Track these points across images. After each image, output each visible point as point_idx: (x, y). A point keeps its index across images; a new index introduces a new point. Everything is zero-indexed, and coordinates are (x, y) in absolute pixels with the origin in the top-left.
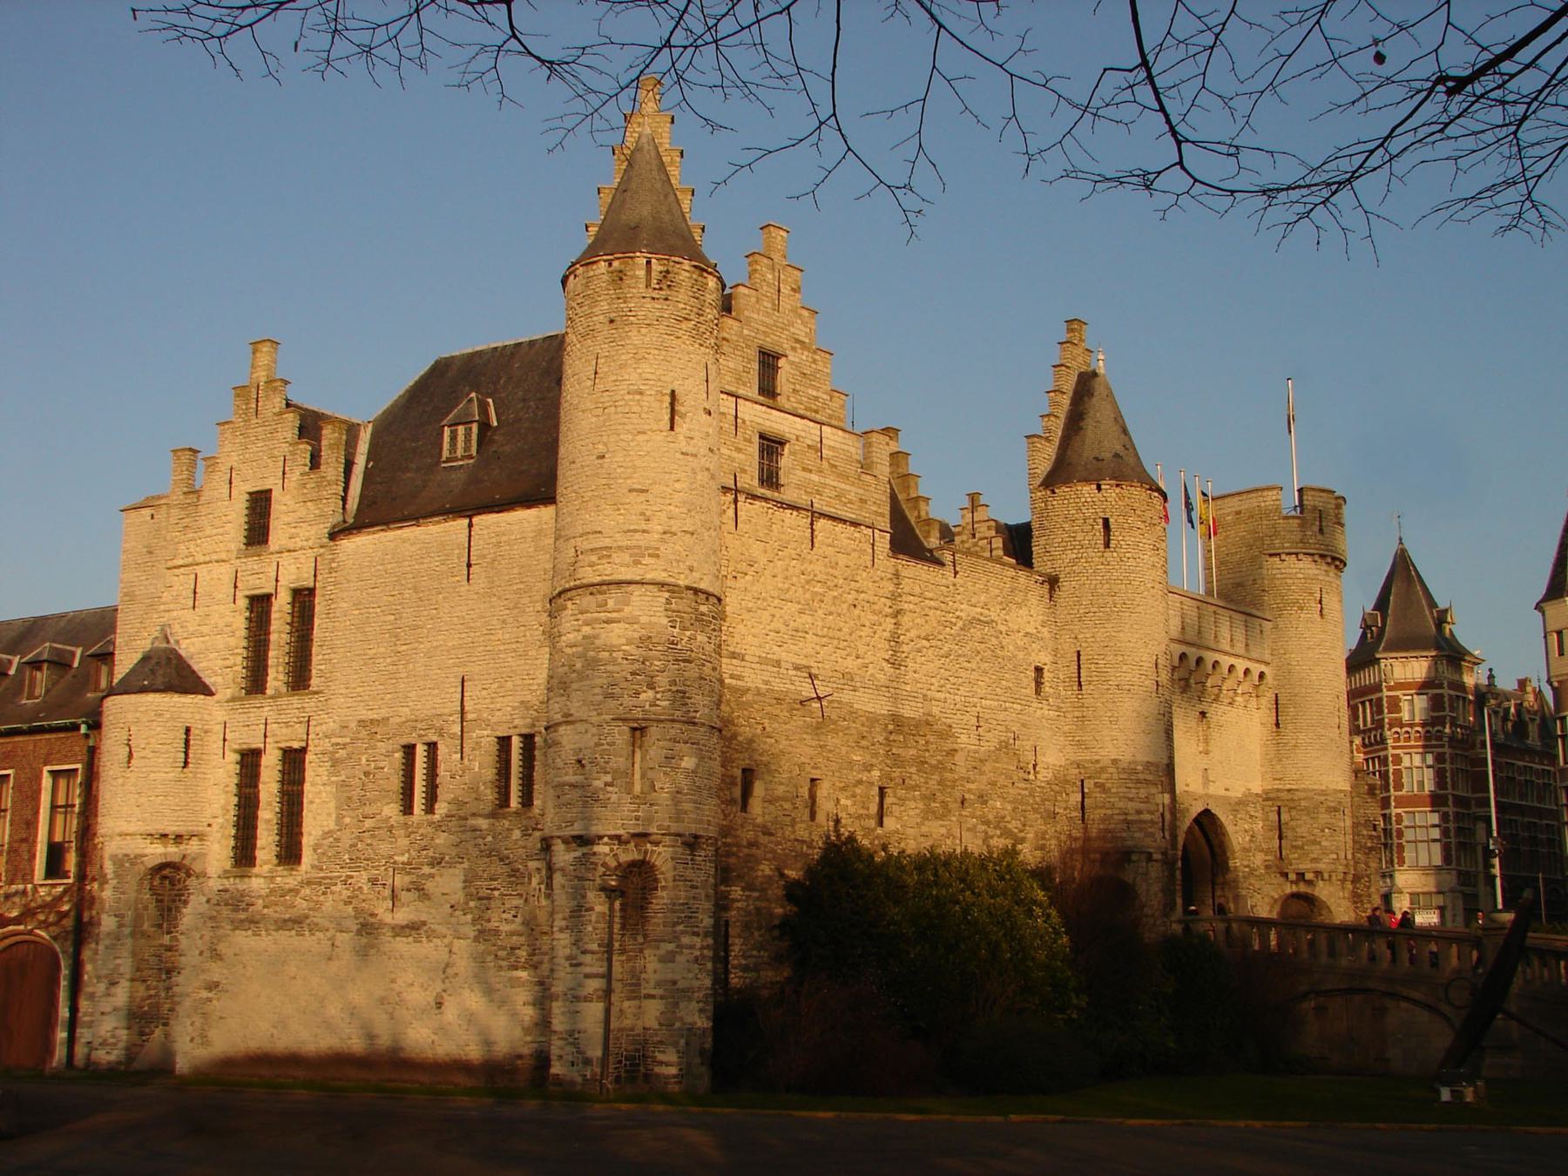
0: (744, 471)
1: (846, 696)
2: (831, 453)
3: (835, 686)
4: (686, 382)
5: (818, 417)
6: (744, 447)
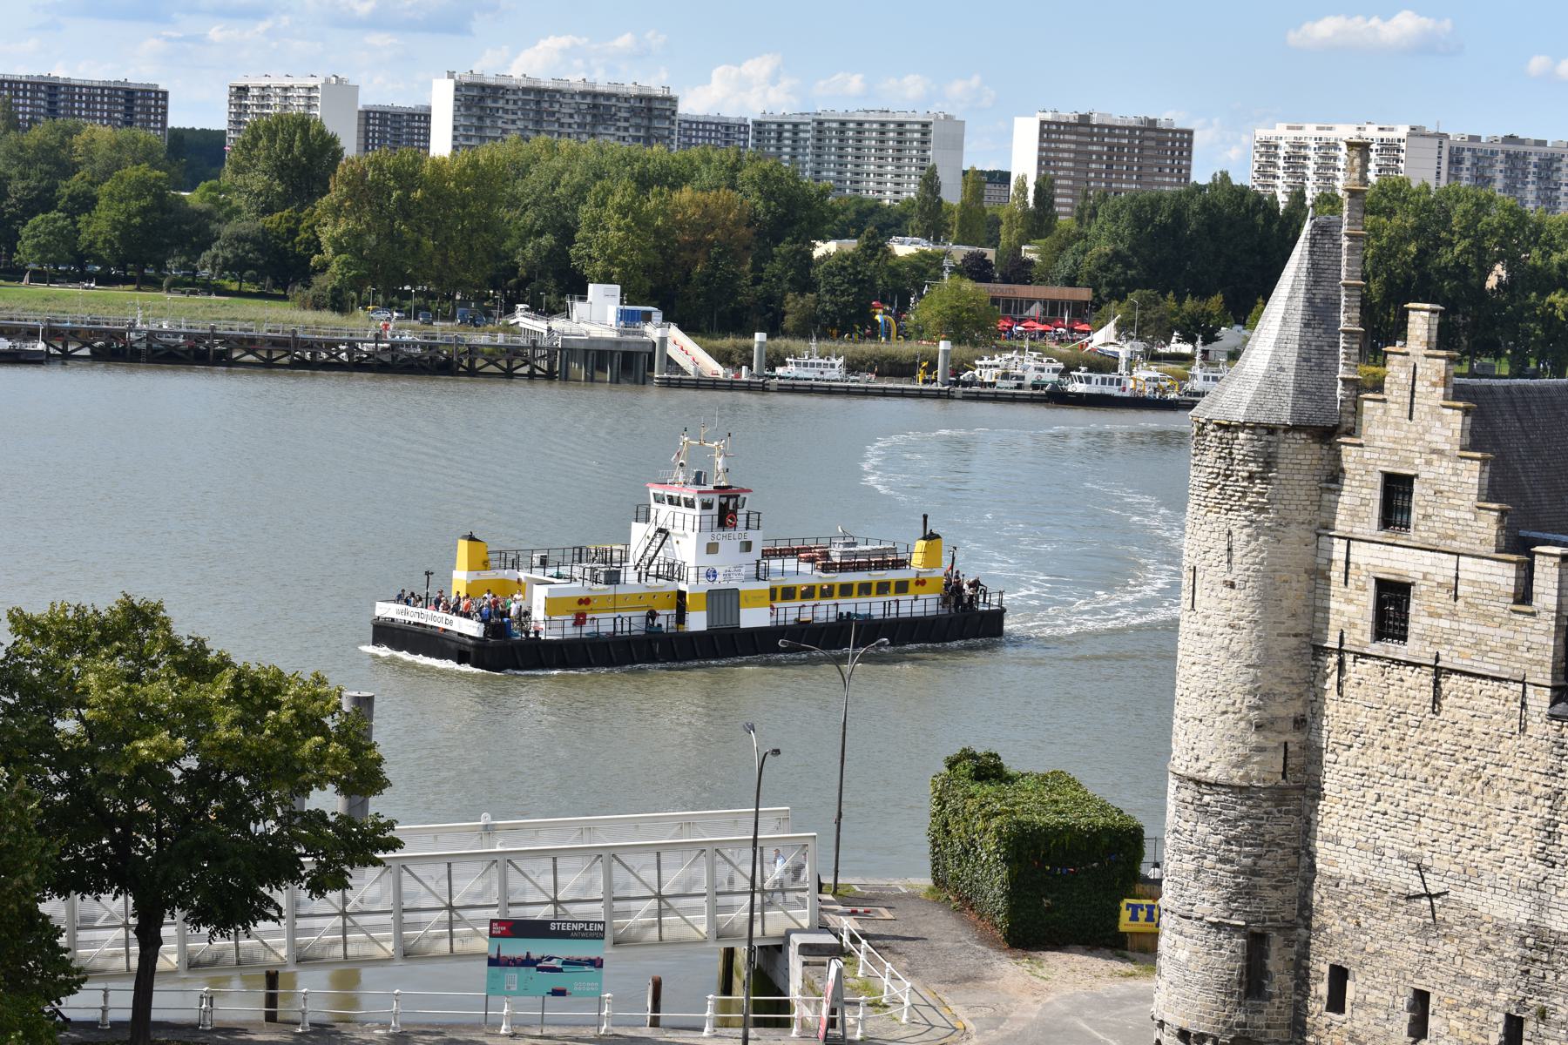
0: (1353, 625)
1: (1468, 896)
2: (1471, 589)
3: (1453, 881)
4: (1208, 556)
5: (1456, 545)
6: (1355, 597)
